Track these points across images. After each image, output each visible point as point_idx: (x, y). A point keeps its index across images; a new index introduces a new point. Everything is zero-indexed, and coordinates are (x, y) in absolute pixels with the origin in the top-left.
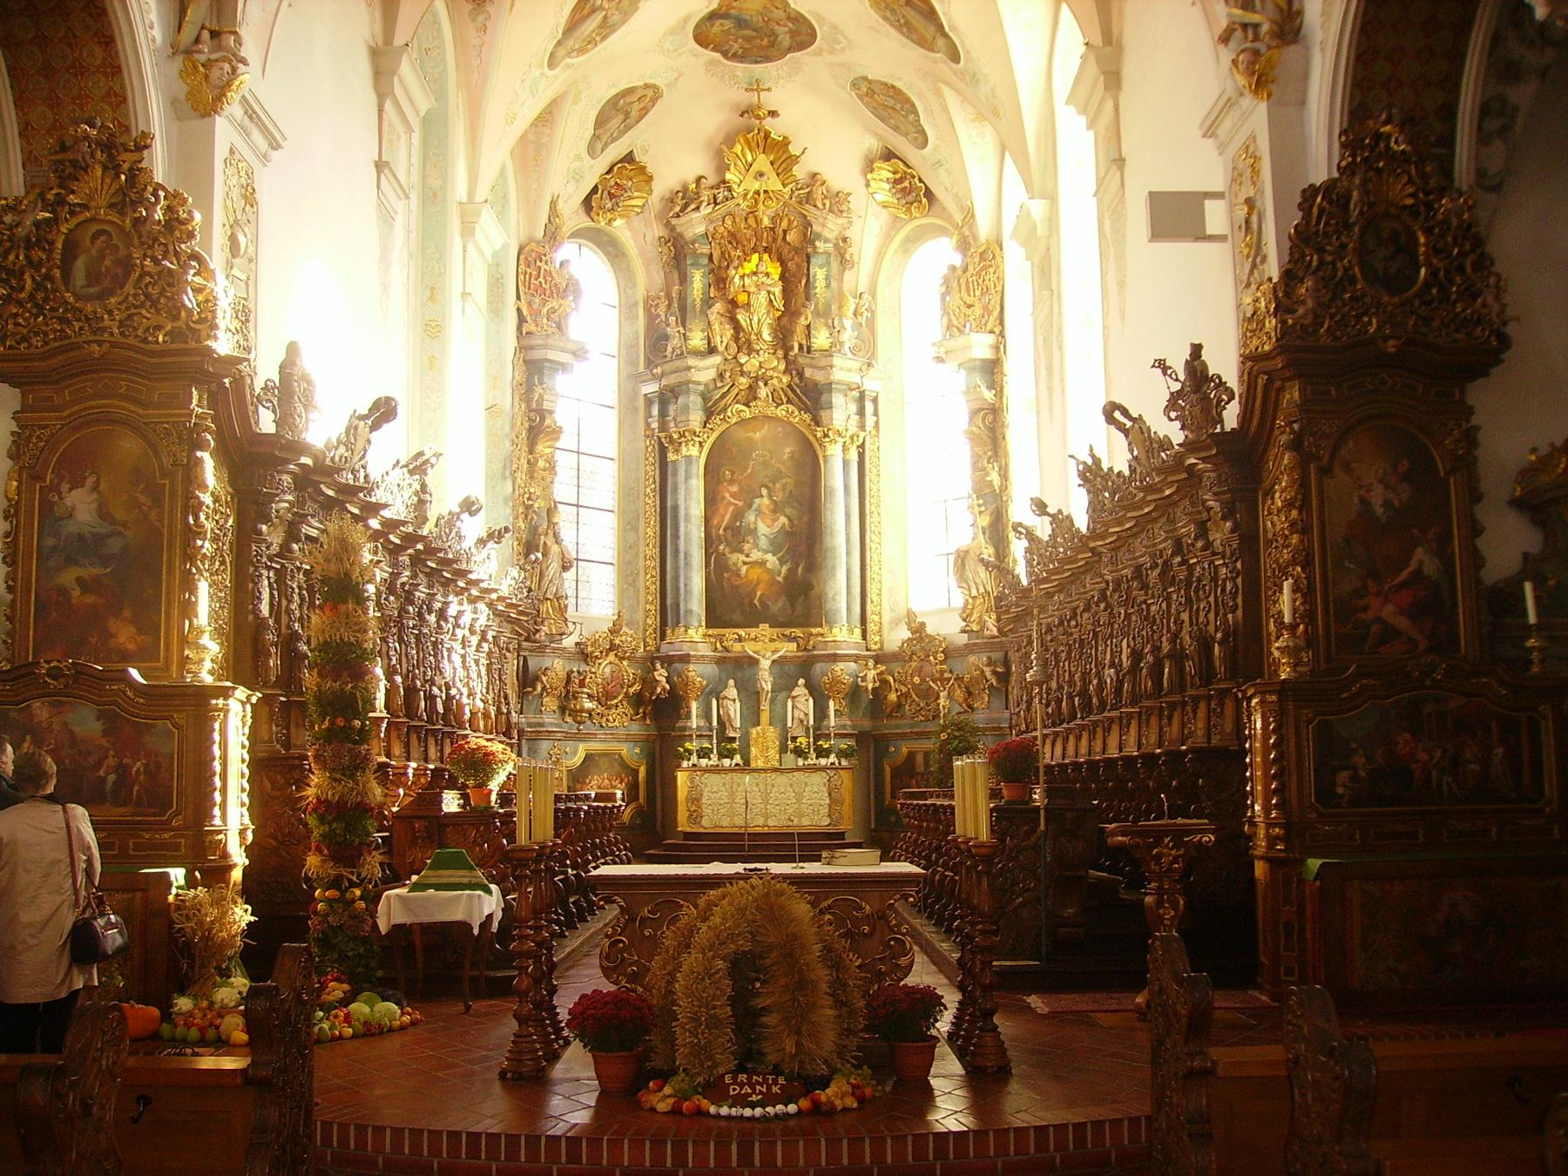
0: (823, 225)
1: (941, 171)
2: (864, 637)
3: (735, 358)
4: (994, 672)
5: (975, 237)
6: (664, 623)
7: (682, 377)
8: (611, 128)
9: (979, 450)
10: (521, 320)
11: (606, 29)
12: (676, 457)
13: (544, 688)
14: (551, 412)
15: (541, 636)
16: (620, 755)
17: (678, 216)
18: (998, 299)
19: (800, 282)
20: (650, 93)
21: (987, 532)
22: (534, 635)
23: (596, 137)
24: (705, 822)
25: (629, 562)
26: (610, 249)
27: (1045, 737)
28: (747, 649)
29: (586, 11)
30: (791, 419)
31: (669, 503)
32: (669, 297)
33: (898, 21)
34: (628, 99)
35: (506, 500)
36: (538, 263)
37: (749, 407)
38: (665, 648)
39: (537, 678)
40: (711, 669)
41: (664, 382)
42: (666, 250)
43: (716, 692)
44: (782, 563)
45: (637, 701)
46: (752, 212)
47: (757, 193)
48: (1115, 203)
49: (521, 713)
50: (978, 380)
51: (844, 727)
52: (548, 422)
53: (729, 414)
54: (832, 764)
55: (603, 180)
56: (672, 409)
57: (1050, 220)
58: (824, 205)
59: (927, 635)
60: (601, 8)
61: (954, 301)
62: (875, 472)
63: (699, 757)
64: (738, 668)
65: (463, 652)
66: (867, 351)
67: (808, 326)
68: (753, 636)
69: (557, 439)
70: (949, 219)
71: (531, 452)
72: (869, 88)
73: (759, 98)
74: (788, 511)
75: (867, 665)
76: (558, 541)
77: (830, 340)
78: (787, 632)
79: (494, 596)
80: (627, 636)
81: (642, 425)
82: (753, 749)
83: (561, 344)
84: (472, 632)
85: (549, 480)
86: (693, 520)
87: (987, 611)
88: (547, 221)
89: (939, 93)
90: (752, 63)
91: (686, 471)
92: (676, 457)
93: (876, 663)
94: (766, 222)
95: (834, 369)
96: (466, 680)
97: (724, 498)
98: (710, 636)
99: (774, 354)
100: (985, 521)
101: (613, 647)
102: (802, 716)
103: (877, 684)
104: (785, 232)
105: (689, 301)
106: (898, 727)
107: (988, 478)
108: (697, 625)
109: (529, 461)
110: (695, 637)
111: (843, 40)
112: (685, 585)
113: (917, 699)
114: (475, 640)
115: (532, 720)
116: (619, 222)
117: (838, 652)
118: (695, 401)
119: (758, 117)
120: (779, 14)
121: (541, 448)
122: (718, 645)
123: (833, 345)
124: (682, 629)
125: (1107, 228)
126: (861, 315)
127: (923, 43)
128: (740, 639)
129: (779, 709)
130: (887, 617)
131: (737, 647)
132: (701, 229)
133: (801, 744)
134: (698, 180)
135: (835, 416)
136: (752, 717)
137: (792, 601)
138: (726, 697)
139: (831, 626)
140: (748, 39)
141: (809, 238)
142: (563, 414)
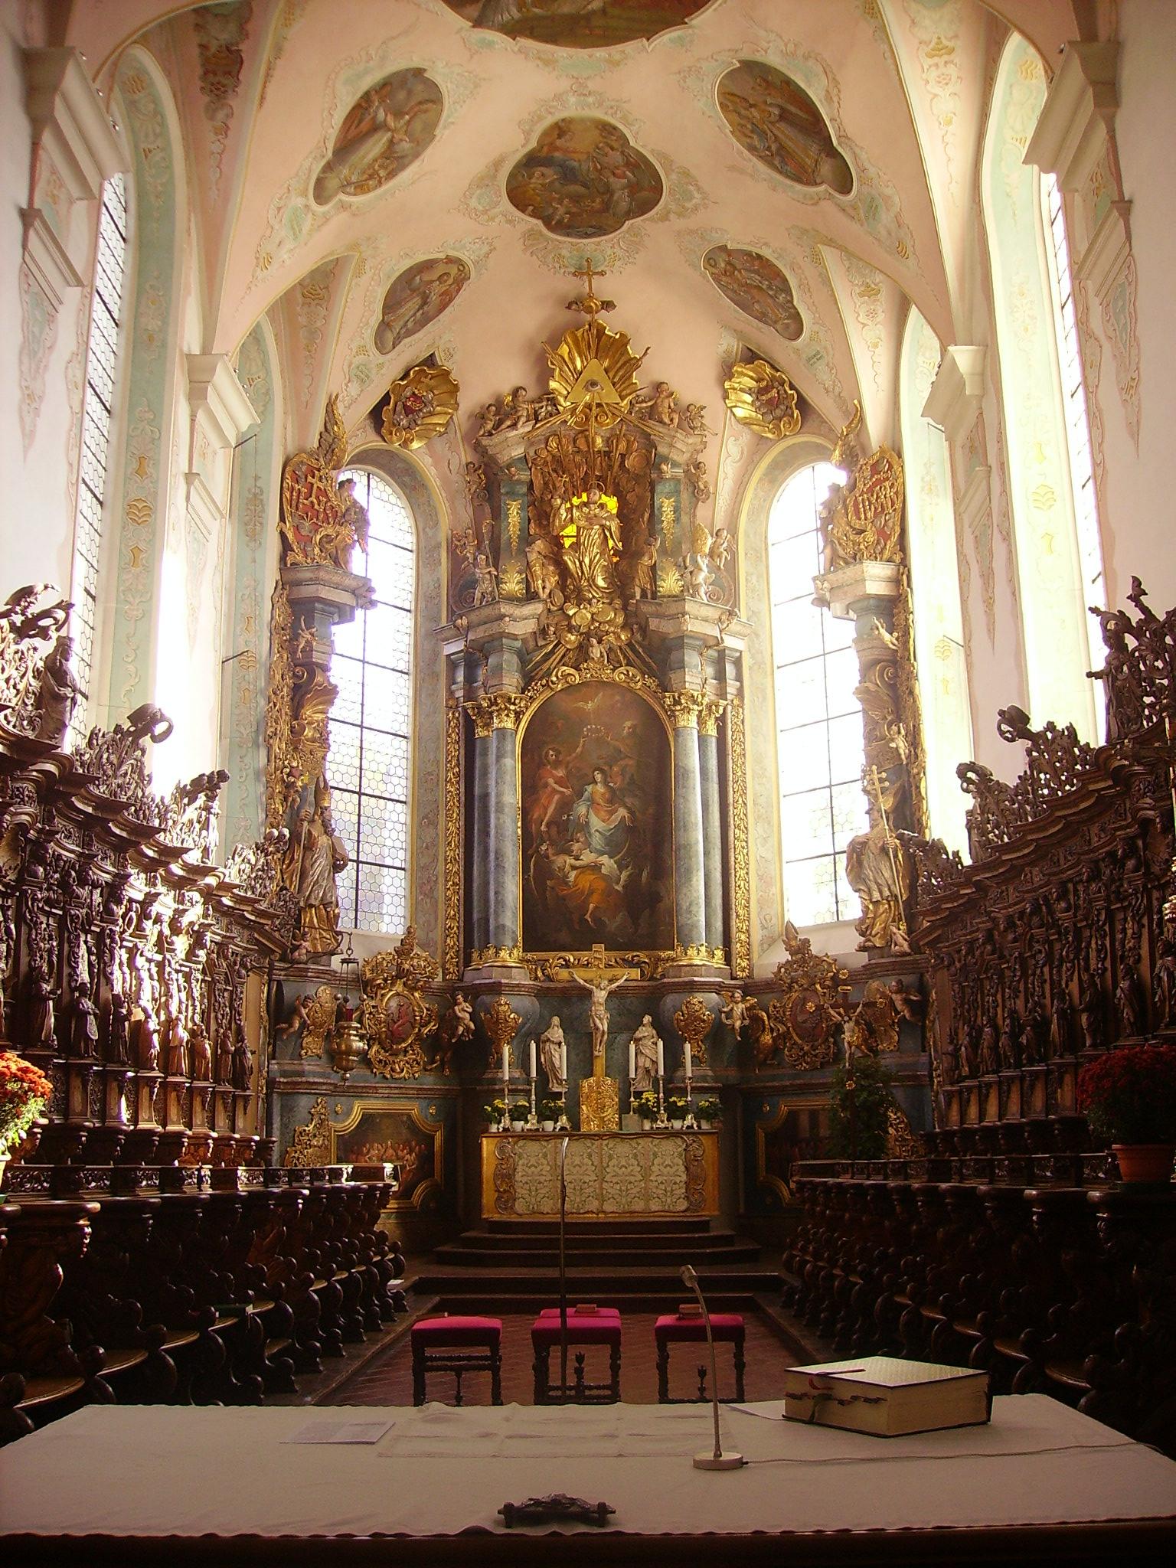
0: (671, 446)
1: (821, 366)
3: (561, 609)
4: (907, 1001)
5: (864, 449)
7: (494, 628)
8: (404, 315)
9: (876, 715)
11: (393, 162)
12: (486, 733)
13: (304, 1025)
14: (325, 669)
15: (301, 955)
16: (409, 1116)
17: (491, 434)
18: (898, 518)
19: (642, 516)
20: (454, 270)
21: (891, 817)
22: (292, 952)
23: (384, 325)
24: (520, 1206)
26: (406, 479)
27: (949, 1096)
28: (575, 976)
29: (365, 126)
30: (633, 685)
31: (477, 791)
32: (478, 536)
33: (769, 148)
34: (426, 277)
35: (257, 774)
36: (310, 479)
37: (577, 669)
38: (469, 976)
39: (294, 1011)
40: (528, 1003)
41: (471, 637)
42: (476, 479)
43: (535, 1032)
44: (621, 868)
45: (432, 1045)
46: (582, 432)
47: (589, 406)
48: (1117, 267)
49: (274, 1059)
51: (704, 1078)
52: (319, 679)
53: (554, 679)
54: (690, 1127)
55: (395, 387)
56: (481, 673)
57: (982, 374)
58: (672, 420)
59: (812, 957)
60: (384, 126)
61: (839, 529)
62: (738, 751)
63: (513, 1119)
65: (159, 957)
66: (726, 594)
67: (653, 568)
68: (584, 960)
69: (331, 702)
70: (829, 431)
71: (296, 715)
72: (729, 263)
73: (590, 288)
74: (628, 800)
75: (733, 996)
76: (328, 830)
77: (680, 583)
78: (629, 956)
79: (211, 880)
81: (443, 694)
82: (584, 1107)
83: (336, 579)
84: (175, 929)
85: (320, 754)
86: (506, 810)
87: (894, 921)
88: (323, 430)
89: (817, 260)
90: (581, 237)
91: (498, 748)
92: (486, 733)
93: (745, 995)
94: (599, 440)
95: (687, 617)
96: (163, 999)
97: (546, 785)
98: (528, 961)
99: (610, 604)
100: (886, 803)
101: (401, 974)
102: (648, 1064)
103: (747, 1022)
104: (623, 456)
105: (504, 537)
106: (774, 1078)
107: (893, 745)
108: (510, 944)
109: (292, 728)
111: (696, 195)
112: (496, 893)
113: (800, 1042)
114: (182, 943)
115: (286, 1068)
116: (415, 445)
117: (696, 979)
118: (510, 661)
119: (589, 310)
120: (616, 158)
121: (307, 711)
122: (539, 974)
123: (685, 589)
124: (492, 951)
125: (1096, 324)
126: (719, 556)
127: (803, 176)
128: (567, 965)
129: (617, 1055)
130: (757, 936)
131: (564, 974)
132: (518, 452)
133: (648, 1100)
134: (515, 392)
135: (687, 678)
136: (583, 1065)
137: (634, 915)
138: (548, 1040)
139: (686, 944)
140: (576, 199)
141: (653, 461)
142: (340, 673)
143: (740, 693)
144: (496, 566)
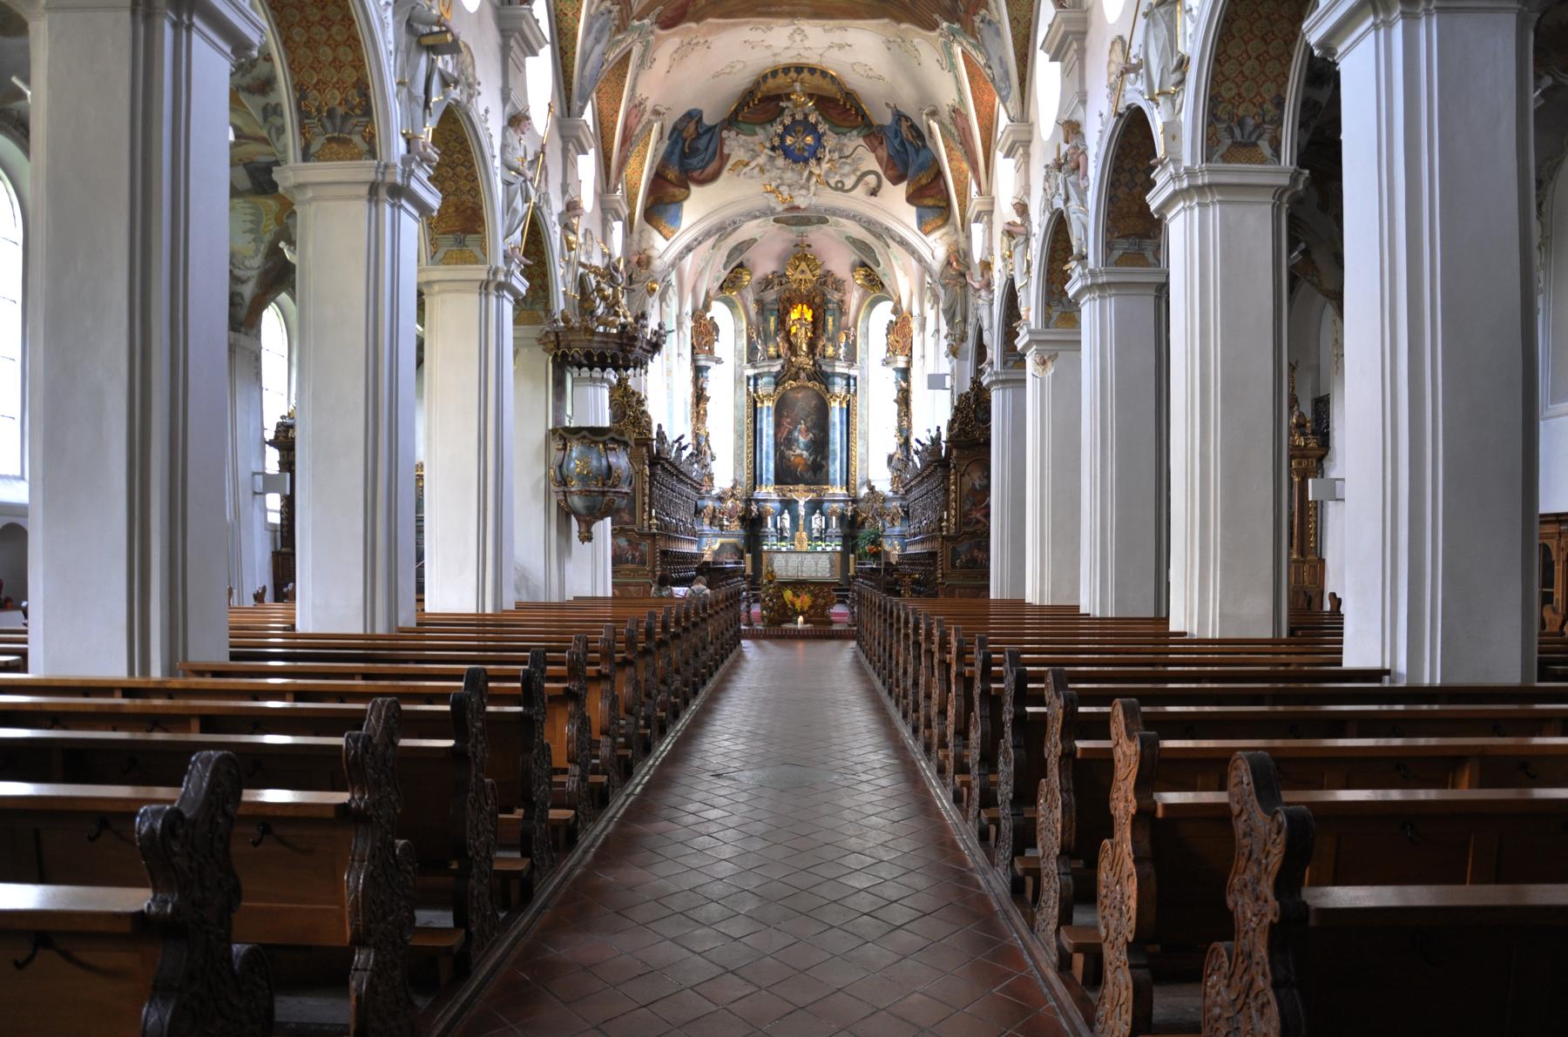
2: (848, 490)
6: (755, 483)
10: (693, 347)
23: (727, 262)
25: (739, 455)
31: (758, 427)
37: (794, 380)
39: (701, 511)
44: (810, 455)
45: (743, 519)
50: (899, 375)
56: (760, 382)
64: (788, 504)
66: (851, 358)
71: (697, 406)
80: (739, 491)
101: (733, 495)
110: (768, 491)
116: (734, 293)
128: (790, 491)
130: (858, 482)
132: (774, 297)
134: (774, 273)
137: (815, 473)
141: (825, 301)
143: (856, 391)
144: (766, 344)
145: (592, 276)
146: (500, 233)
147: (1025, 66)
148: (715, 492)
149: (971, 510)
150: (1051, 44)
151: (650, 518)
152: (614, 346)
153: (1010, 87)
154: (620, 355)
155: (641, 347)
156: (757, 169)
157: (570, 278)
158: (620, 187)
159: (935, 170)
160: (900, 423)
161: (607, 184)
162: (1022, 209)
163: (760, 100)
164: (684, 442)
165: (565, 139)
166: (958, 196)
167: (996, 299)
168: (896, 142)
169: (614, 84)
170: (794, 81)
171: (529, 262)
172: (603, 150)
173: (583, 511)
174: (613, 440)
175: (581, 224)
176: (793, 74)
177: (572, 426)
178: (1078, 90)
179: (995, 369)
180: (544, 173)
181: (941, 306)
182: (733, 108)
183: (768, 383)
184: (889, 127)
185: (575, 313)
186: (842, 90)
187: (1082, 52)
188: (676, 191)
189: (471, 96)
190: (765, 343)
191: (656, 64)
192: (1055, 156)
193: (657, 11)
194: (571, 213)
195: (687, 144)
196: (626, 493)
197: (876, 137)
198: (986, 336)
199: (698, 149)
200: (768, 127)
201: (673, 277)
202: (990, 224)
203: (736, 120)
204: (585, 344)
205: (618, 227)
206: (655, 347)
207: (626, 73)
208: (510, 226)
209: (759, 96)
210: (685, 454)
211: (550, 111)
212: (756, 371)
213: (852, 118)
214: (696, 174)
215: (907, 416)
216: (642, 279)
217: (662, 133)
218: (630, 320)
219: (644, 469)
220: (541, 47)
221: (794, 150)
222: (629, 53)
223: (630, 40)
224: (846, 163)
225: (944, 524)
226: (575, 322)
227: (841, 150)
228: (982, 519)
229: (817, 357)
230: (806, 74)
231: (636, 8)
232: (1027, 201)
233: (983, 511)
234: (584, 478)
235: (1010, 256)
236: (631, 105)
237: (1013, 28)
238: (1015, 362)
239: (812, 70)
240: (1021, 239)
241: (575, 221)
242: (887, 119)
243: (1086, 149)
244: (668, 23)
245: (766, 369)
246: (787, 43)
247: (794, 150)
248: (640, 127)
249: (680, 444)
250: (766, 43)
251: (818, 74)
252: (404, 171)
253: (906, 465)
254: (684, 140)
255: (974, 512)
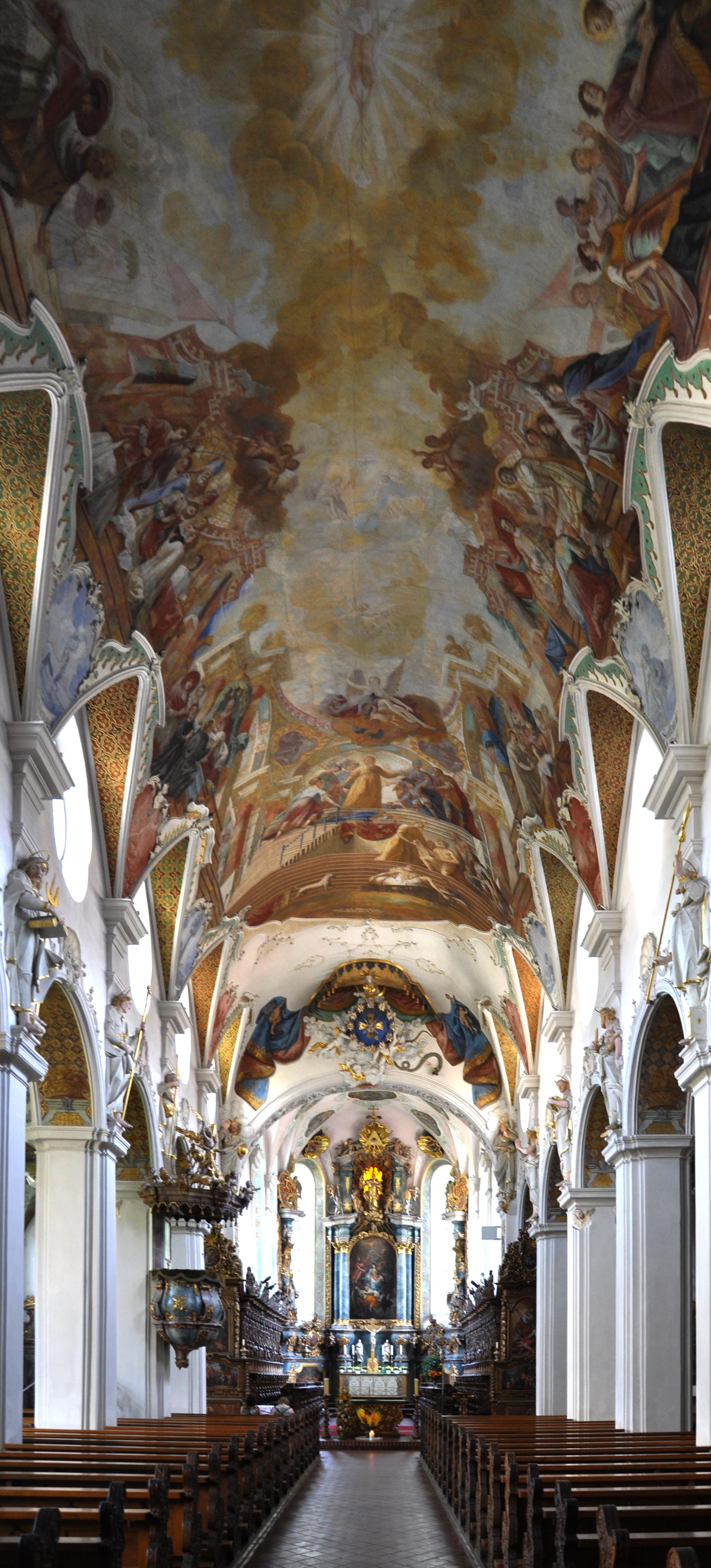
10: (279, 1202)
66: (416, 1213)
145: (188, 1139)
146: (104, 1099)
147: (567, 961)
148: (298, 1324)
149: (518, 1341)
150: (590, 941)
151: (241, 1346)
152: (207, 1201)
153: (554, 980)
154: (212, 1208)
155: (231, 1203)
156: (334, 1051)
157: (168, 1141)
158: (213, 1062)
159: (488, 1053)
160: (458, 1267)
161: (202, 1060)
162: (565, 1086)
163: (336, 990)
164: (270, 1283)
165: (164, 1019)
166: (508, 1075)
167: (541, 1163)
168: (455, 1029)
169: (208, 973)
170: (366, 974)
171: (129, 1125)
172: (198, 1029)
173: (180, 1342)
174: (206, 1281)
175: (178, 1095)
176: (365, 968)
177: (170, 1268)
178: (613, 981)
179: (540, 1222)
180: (144, 1048)
181: (493, 1169)
182: (313, 997)
183: (344, 1234)
184: (449, 1015)
185: (172, 1172)
186: (408, 982)
187: (617, 948)
188: (264, 1068)
189: (76, 977)
190: (342, 1199)
191: (245, 957)
192: (594, 1039)
193: (246, 909)
194: (169, 1085)
195: (273, 1027)
196: (218, 1327)
197: (438, 1024)
198: (532, 1194)
199: (282, 1032)
200: (344, 1014)
201: (261, 1142)
202: (536, 1098)
203: (316, 1008)
204: (182, 1198)
205: (212, 1098)
206: (243, 1202)
207: (218, 964)
208: (113, 1094)
209: (336, 987)
210: (272, 1293)
211: (149, 993)
212: (334, 1223)
213: (417, 1007)
214: (280, 1054)
215: (463, 1261)
216: (233, 1143)
217: (250, 1017)
218: (221, 1178)
219: (235, 1305)
220: (141, 936)
221: (366, 1034)
222: (221, 946)
223: (221, 934)
224: (411, 1046)
225: (496, 1352)
226: (173, 1179)
227: (407, 1035)
228: (529, 1348)
229: (387, 1212)
230: (376, 969)
231: (227, 907)
232: (568, 1079)
233: (530, 1342)
234: (180, 1313)
235: (554, 1127)
236: (223, 992)
237: (556, 928)
238: (558, 1216)
239: (382, 965)
240: (563, 1111)
241: (172, 1091)
242: (447, 1008)
243: (621, 1033)
244: (256, 920)
245: (342, 1222)
246: (360, 941)
247: (366, 1034)
248: (231, 1011)
249: (267, 1284)
250: (342, 941)
251: (387, 968)
252: (12, 1040)
253: (463, 1303)
254: (270, 1024)
255: (522, 1343)
